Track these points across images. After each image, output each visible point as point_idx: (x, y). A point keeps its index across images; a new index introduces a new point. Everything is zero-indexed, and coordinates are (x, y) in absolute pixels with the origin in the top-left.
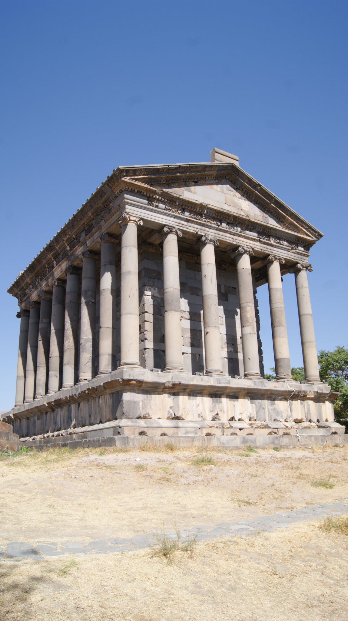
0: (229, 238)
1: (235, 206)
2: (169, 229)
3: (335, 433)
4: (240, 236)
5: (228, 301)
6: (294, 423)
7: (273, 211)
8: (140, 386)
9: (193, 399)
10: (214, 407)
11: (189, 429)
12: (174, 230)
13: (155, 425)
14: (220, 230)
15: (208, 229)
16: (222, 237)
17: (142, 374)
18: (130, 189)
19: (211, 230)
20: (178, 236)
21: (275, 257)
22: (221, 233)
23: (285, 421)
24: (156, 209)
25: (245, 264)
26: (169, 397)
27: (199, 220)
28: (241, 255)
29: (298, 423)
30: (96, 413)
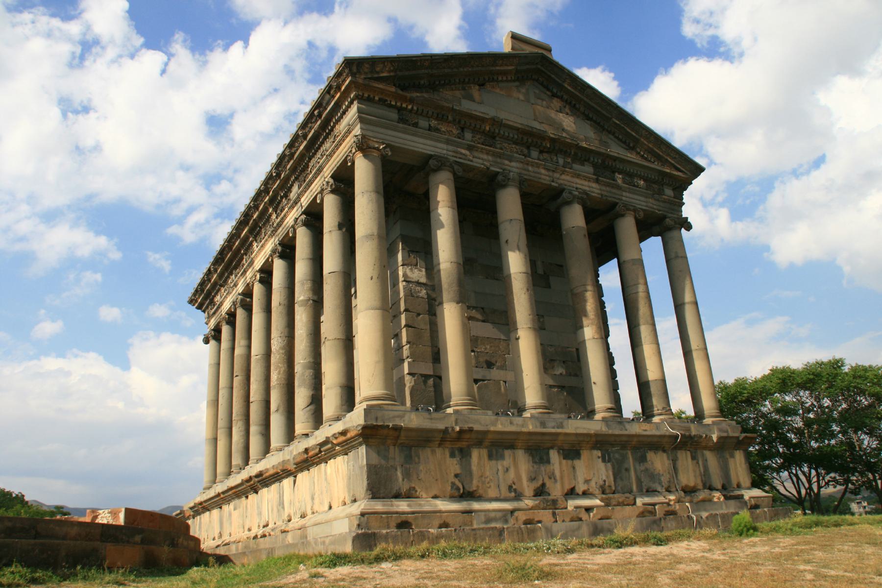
0: (544, 176)
1: (552, 123)
3: (756, 507)
4: (563, 173)
5: (550, 287)
6: (682, 494)
8: (398, 437)
9: (497, 460)
11: (493, 515)
12: (448, 164)
13: (427, 508)
15: (507, 162)
16: (532, 174)
17: (398, 417)
18: (366, 95)
19: (513, 164)
20: (454, 174)
21: (625, 206)
22: (530, 168)
24: (414, 129)
25: (574, 218)
26: (452, 455)
27: (490, 146)
28: (569, 203)
30: (322, 493)
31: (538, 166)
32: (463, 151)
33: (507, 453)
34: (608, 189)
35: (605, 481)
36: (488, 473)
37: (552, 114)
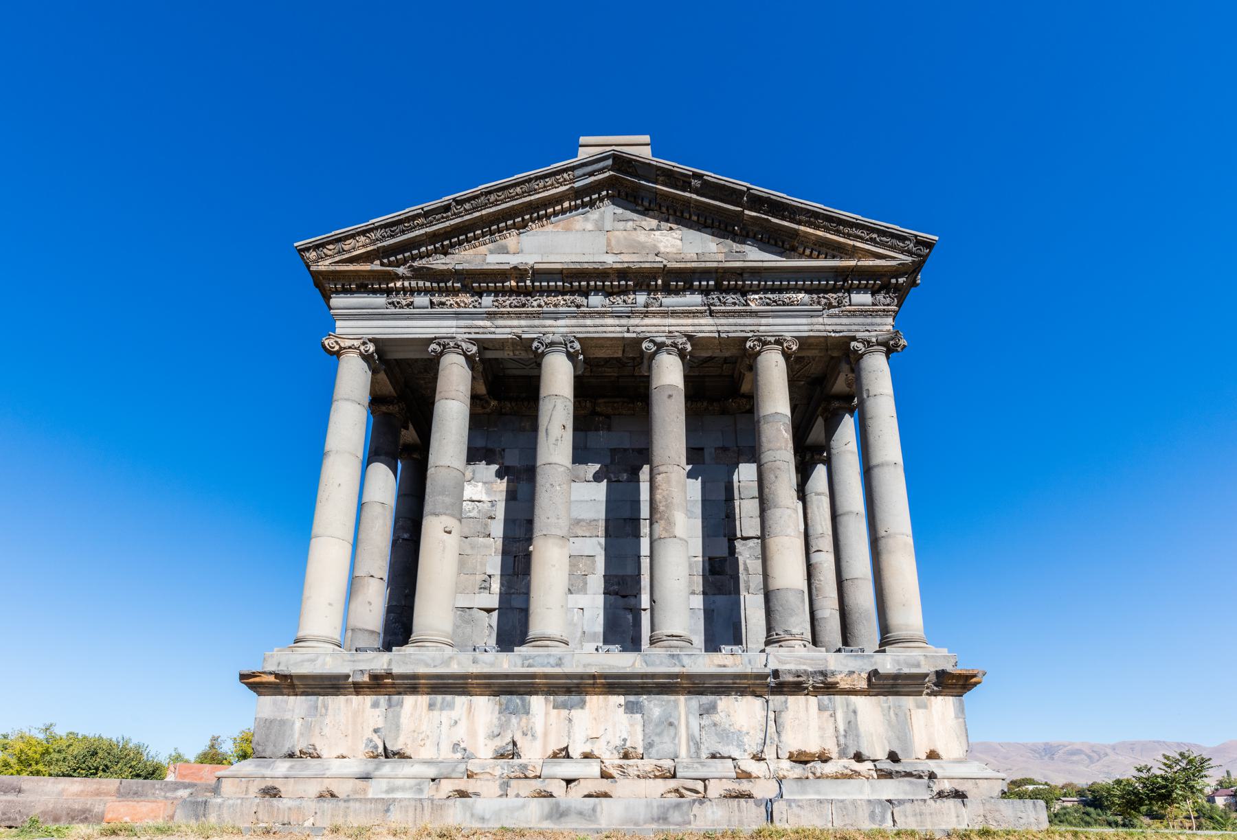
0: (611, 328)
1: (637, 248)
2: (439, 344)
4: (646, 315)
6: (786, 764)
7: (756, 229)
9: (442, 709)
10: (503, 726)
11: (399, 782)
12: (452, 344)
14: (585, 315)
17: (309, 660)
19: (560, 322)
20: (465, 355)
22: (589, 322)
23: (758, 758)
26: (375, 705)
27: (524, 305)
29: (806, 763)
31: (602, 314)
32: (481, 323)
33: (460, 701)
34: (731, 321)
35: (625, 740)
36: (424, 728)
37: (642, 237)
